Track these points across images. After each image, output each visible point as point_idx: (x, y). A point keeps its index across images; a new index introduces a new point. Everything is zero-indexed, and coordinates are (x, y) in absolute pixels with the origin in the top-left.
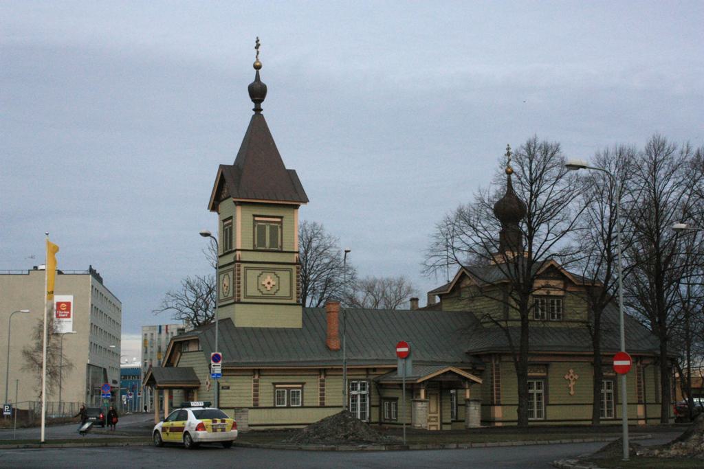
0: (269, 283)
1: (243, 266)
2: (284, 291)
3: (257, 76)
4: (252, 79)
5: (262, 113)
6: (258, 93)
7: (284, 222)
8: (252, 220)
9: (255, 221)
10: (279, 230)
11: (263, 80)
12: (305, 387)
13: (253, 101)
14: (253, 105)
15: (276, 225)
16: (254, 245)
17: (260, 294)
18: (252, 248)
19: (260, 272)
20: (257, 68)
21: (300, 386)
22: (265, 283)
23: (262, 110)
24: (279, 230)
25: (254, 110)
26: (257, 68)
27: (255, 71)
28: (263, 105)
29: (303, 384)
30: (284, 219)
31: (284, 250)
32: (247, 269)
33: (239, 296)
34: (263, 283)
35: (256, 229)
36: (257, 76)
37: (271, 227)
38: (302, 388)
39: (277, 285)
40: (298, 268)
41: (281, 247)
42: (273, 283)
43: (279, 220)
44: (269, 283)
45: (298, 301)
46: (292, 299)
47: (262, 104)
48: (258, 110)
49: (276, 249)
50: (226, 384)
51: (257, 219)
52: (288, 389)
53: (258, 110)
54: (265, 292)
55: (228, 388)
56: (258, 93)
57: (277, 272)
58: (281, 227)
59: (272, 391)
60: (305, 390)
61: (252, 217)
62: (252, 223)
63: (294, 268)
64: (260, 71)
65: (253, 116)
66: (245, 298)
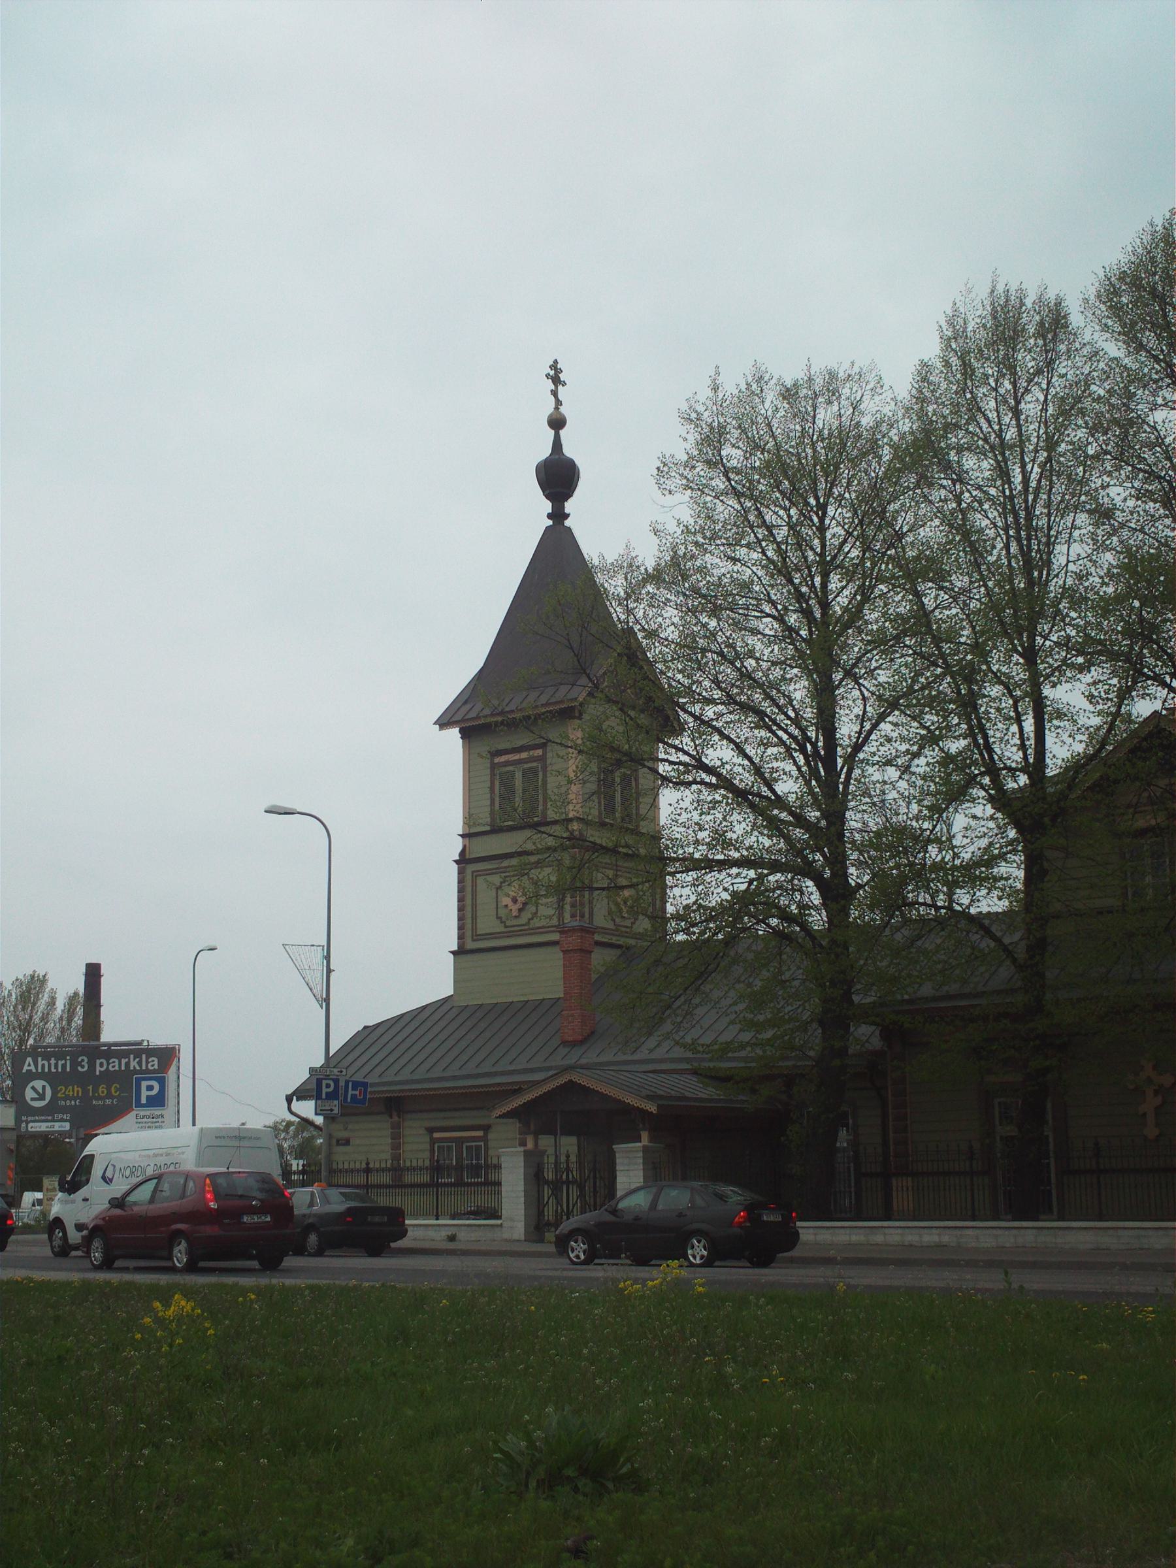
1: (471, 868)
3: (557, 445)
4: (545, 452)
5: (567, 523)
9: (493, 767)
10: (541, 774)
11: (568, 451)
12: (491, 1136)
13: (547, 497)
14: (548, 506)
15: (534, 764)
16: (493, 819)
17: (501, 929)
20: (557, 423)
21: (480, 1133)
23: (567, 516)
25: (550, 516)
26: (557, 423)
27: (552, 432)
28: (569, 506)
29: (486, 1128)
36: (557, 445)
37: (525, 772)
38: (485, 1139)
47: (566, 504)
48: (558, 515)
50: (344, 1134)
51: (497, 760)
52: (460, 1141)
53: (558, 515)
55: (347, 1142)
59: (428, 1146)
66: (473, 940)
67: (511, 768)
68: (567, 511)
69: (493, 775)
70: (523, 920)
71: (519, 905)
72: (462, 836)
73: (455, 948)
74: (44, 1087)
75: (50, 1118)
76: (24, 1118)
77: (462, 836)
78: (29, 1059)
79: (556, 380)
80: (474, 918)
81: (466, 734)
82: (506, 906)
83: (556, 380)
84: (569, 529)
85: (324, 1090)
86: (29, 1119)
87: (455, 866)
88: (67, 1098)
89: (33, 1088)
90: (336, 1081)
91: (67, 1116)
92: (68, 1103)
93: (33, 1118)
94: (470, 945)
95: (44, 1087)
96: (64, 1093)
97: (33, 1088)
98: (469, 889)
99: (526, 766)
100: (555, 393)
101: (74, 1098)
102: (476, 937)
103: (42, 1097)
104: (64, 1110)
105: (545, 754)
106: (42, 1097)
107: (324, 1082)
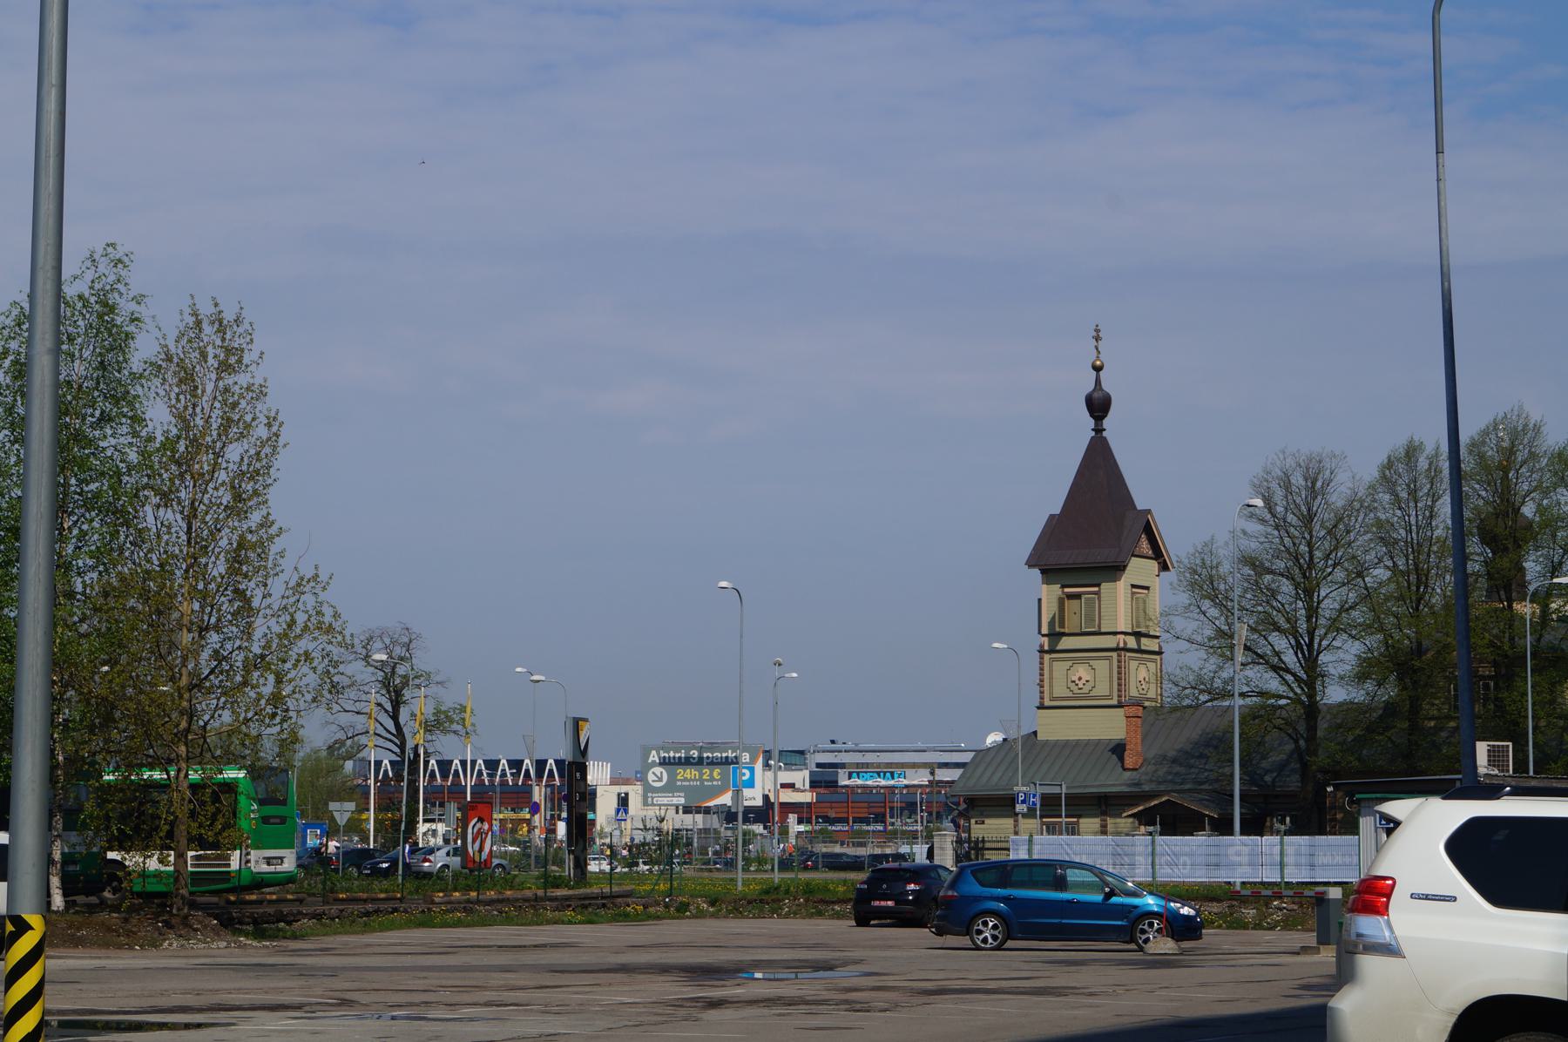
2: (1102, 688)
3: (1098, 381)
5: (1105, 434)
6: (1098, 406)
7: (1102, 591)
10: (1097, 602)
11: (1106, 386)
14: (1091, 422)
19: (1070, 663)
22: (1075, 678)
28: (1106, 423)
31: (1103, 630)
33: (1042, 698)
34: (1073, 679)
36: (1098, 381)
39: (1092, 680)
40: (1119, 656)
41: (1099, 626)
44: (1080, 679)
45: (1119, 702)
47: (1104, 421)
48: (1099, 430)
49: (1093, 630)
53: (1099, 430)
54: (1076, 690)
56: (1098, 406)
58: (1100, 601)
60: (1081, 826)
63: (1114, 655)
64: (1101, 373)
65: (1092, 437)
68: (1104, 427)
70: (1085, 690)
71: (1083, 681)
74: (661, 773)
75: (670, 795)
76: (650, 795)
78: (654, 752)
79: (1097, 339)
80: (1051, 686)
81: (1043, 572)
82: (1074, 682)
83: (1097, 339)
84: (1105, 438)
85: (1020, 799)
86: (654, 795)
88: (685, 779)
89: (653, 773)
90: (1025, 794)
91: (682, 794)
92: (684, 783)
93: (657, 795)
94: (1047, 703)
95: (661, 773)
96: (683, 776)
97: (653, 773)
98: (1046, 672)
100: (1097, 348)
101: (695, 780)
103: (660, 780)
104: (680, 789)
105: (1099, 591)
106: (660, 780)
107: (1020, 795)
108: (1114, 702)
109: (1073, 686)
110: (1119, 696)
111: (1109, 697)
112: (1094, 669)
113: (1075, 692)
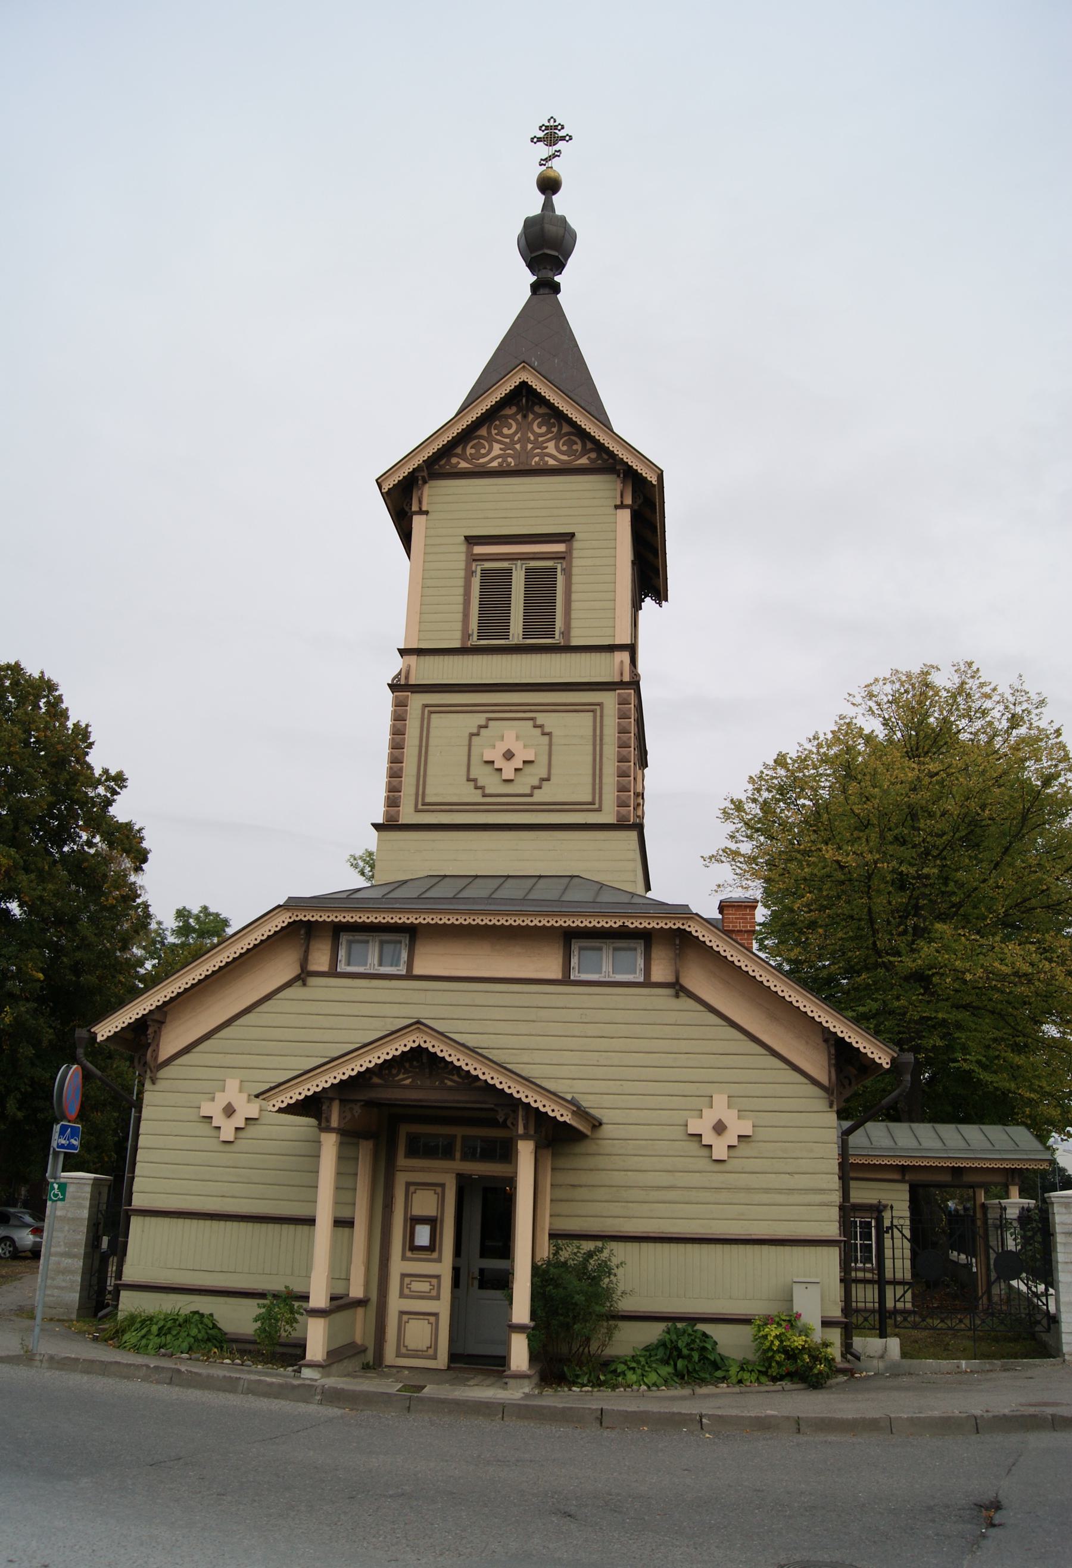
0: (509, 755)
1: (416, 702)
3: (548, 206)
7: (575, 554)
8: (463, 557)
15: (549, 564)
16: (466, 635)
18: (458, 645)
19: (481, 719)
20: (549, 185)
22: (495, 755)
24: (560, 579)
26: (549, 185)
30: (576, 544)
31: (575, 642)
32: (430, 710)
35: (476, 582)
36: (548, 206)
40: (623, 702)
41: (566, 633)
42: (522, 754)
43: (560, 548)
44: (509, 755)
46: (599, 810)
51: (478, 550)
54: (493, 785)
57: (541, 718)
58: (568, 573)
61: (463, 548)
62: (462, 565)
64: (555, 198)
67: (505, 565)
69: (469, 574)
70: (522, 786)
72: (403, 652)
73: (380, 820)
77: (403, 652)
82: (493, 762)
87: (389, 695)
94: (407, 815)
99: (533, 564)
102: (423, 805)
105: (569, 551)
108: (611, 819)
109: (478, 771)
110: (622, 804)
111: (594, 806)
112: (549, 734)
113: (487, 791)
